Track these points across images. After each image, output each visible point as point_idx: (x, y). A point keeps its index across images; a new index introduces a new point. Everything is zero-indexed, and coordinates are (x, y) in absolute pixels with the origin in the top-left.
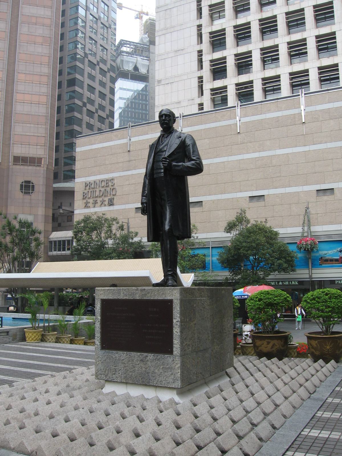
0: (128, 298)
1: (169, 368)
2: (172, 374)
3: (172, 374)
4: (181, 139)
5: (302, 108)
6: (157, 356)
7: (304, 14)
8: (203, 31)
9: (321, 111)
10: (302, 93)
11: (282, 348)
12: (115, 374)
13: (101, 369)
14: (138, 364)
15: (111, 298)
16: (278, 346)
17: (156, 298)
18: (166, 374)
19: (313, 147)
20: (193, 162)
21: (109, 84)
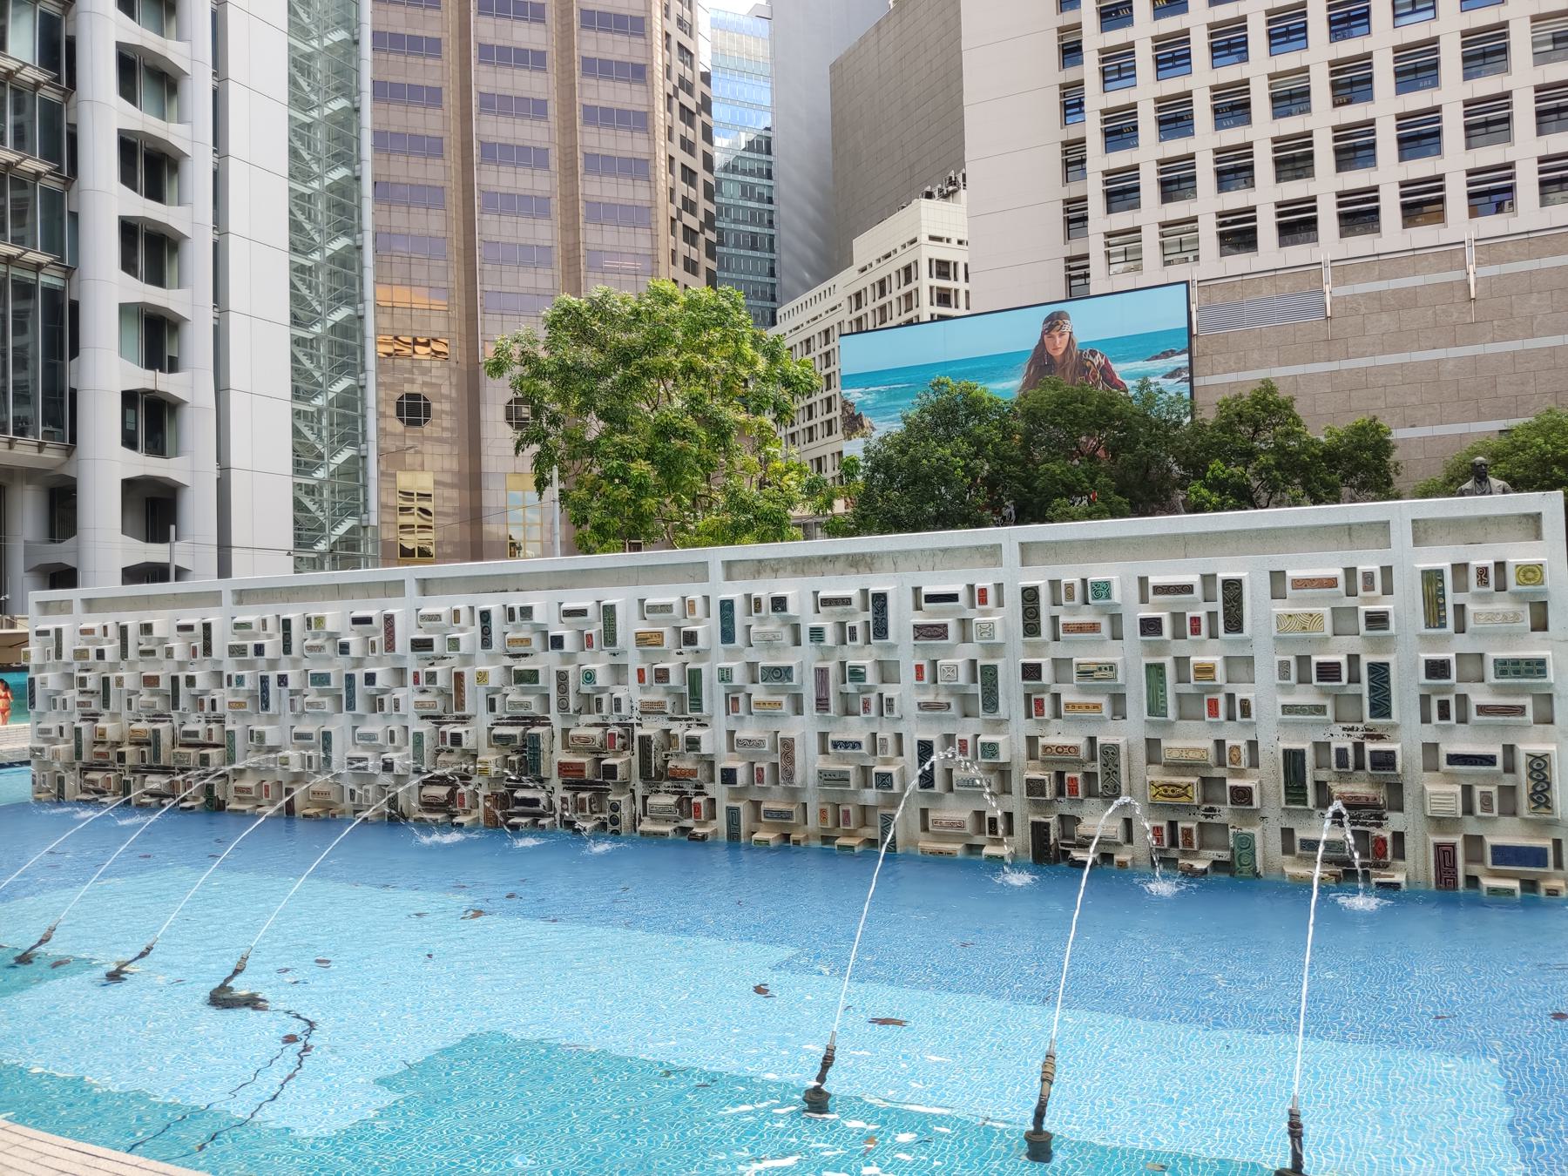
9: (1363, 295)
19: (1346, 364)
21: (701, 146)
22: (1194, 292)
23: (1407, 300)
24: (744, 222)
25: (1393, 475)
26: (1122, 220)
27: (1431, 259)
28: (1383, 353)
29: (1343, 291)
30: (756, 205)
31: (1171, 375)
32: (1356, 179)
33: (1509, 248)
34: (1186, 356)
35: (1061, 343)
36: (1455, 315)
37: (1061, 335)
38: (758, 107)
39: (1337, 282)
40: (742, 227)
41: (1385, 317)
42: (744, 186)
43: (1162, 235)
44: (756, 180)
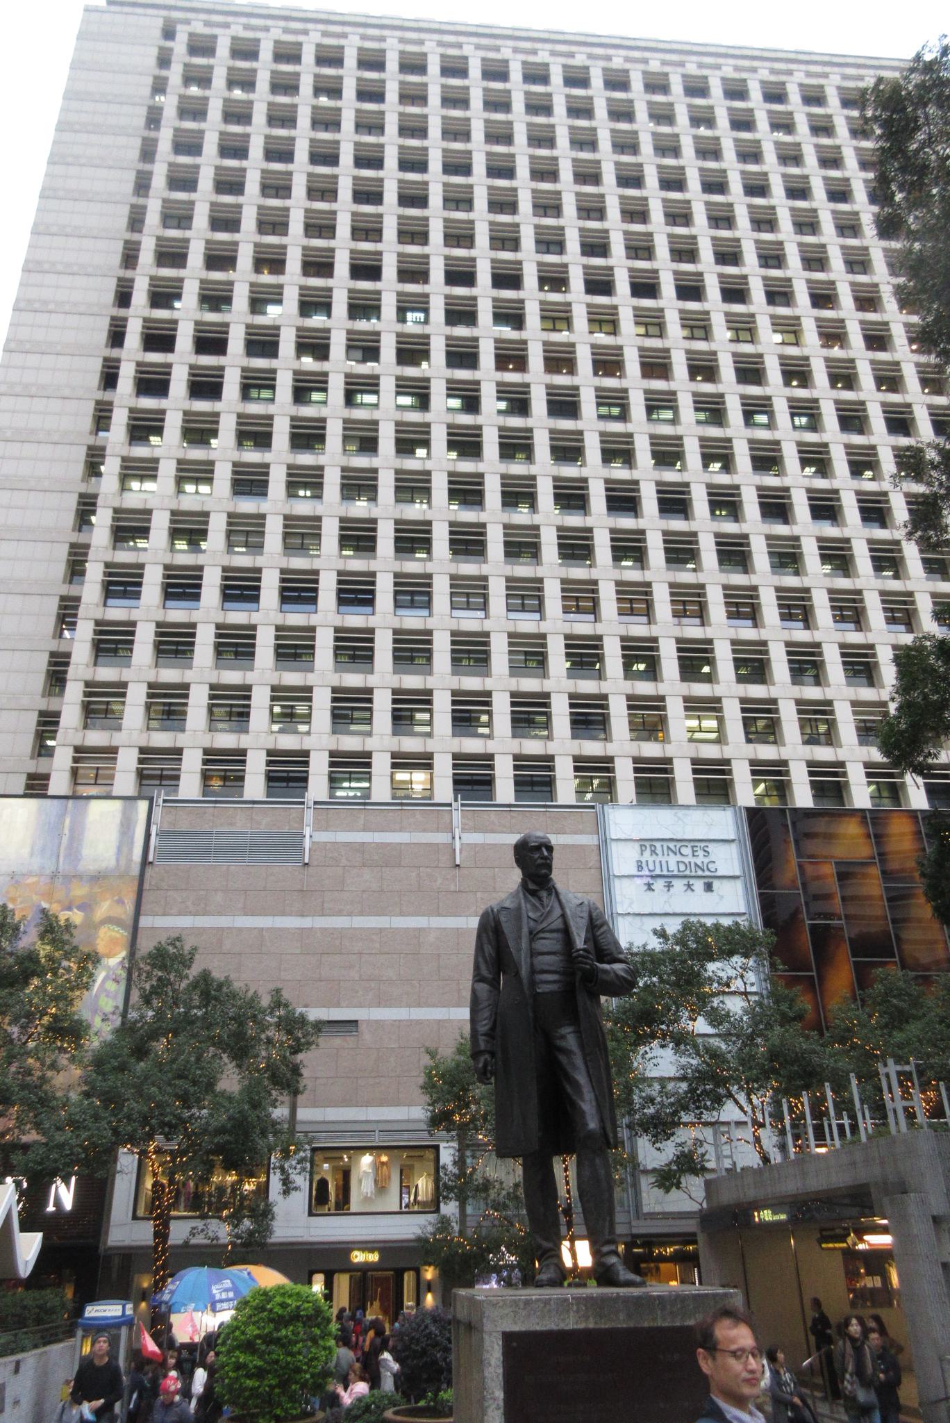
0: (591, 1326)
15: (538, 1328)
23: (390, 857)
27: (418, 816)
28: (361, 914)
29: (324, 837)
36: (439, 881)
39: (318, 827)
41: (367, 874)
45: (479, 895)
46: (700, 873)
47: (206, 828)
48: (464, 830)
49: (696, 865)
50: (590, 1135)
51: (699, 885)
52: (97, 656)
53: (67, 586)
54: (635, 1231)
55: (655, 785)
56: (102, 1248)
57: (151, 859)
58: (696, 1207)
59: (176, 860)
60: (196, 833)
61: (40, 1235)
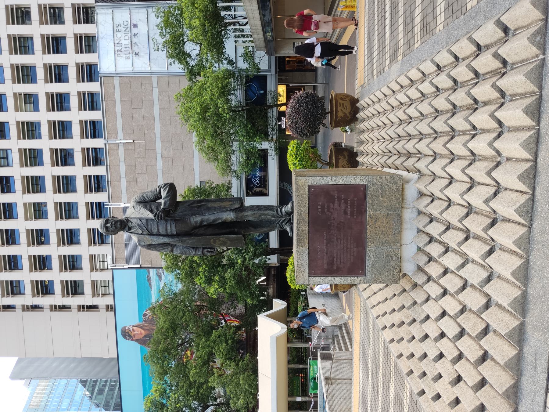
1: (381, 189)
2: (388, 185)
3: (388, 185)
4: (135, 206)
5: (118, 141)
6: (369, 203)
7: (30, 204)
8: (30, 303)
10: (108, 205)
11: (347, 158)
12: (392, 258)
13: (388, 276)
14: (379, 227)
16: (344, 162)
17: (307, 206)
18: (388, 193)
20: (162, 190)
22: (118, 266)
24: (113, 393)
25: (213, 185)
26: (88, 288)
27: (112, 158)
30: (107, 388)
31: (160, 277)
32: (80, 184)
33: (110, 125)
34: (151, 271)
35: (138, 331)
37: (134, 331)
38: (66, 385)
39: (120, 200)
40: (115, 395)
42: (99, 393)
43: (97, 270)
44: (97, 387)
45: (146, 132)
46: (129, 29)
47: (124, 246)
48: (117, 138)
49: (125, 31)
50: (237, 217)
51: (135, 31)
52: (50, 294)
53: (16, 310)
54: (274, 73)
55: (87, 44)
56: (277, 265)
57: (139, 266)
58: (266, 57)
59: (139, 258)
60: (126, 250)
61: (274, 300)
